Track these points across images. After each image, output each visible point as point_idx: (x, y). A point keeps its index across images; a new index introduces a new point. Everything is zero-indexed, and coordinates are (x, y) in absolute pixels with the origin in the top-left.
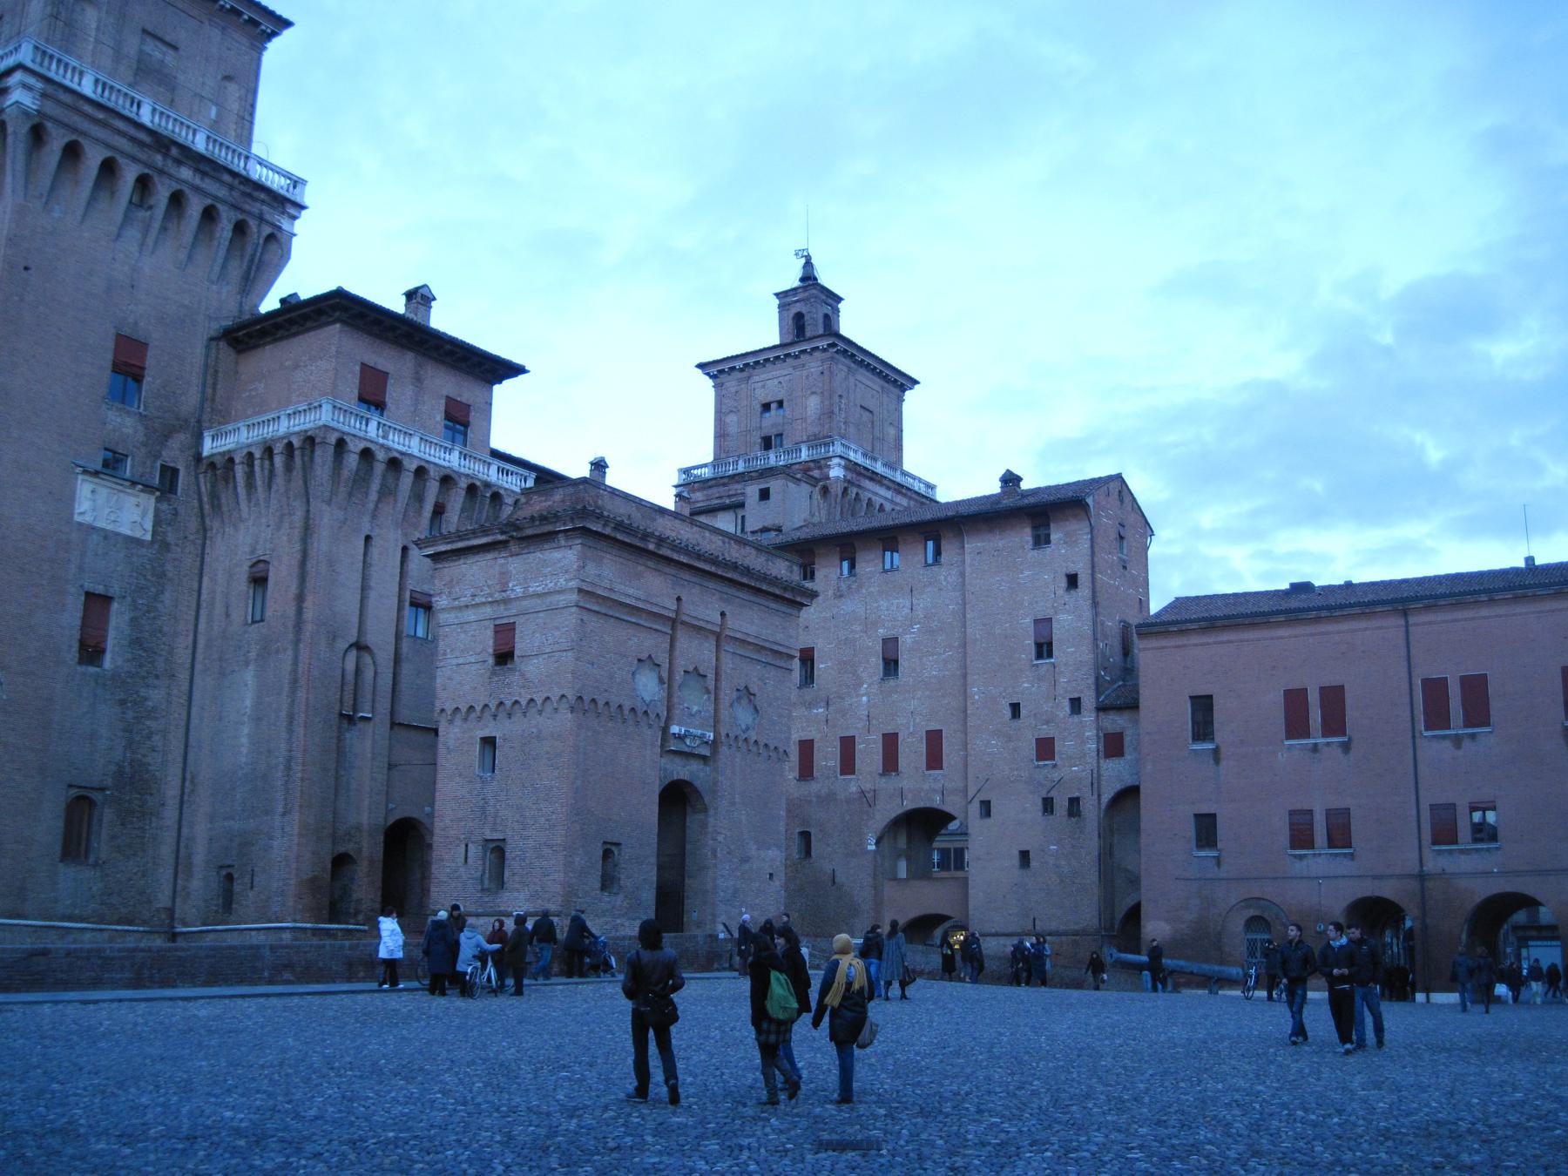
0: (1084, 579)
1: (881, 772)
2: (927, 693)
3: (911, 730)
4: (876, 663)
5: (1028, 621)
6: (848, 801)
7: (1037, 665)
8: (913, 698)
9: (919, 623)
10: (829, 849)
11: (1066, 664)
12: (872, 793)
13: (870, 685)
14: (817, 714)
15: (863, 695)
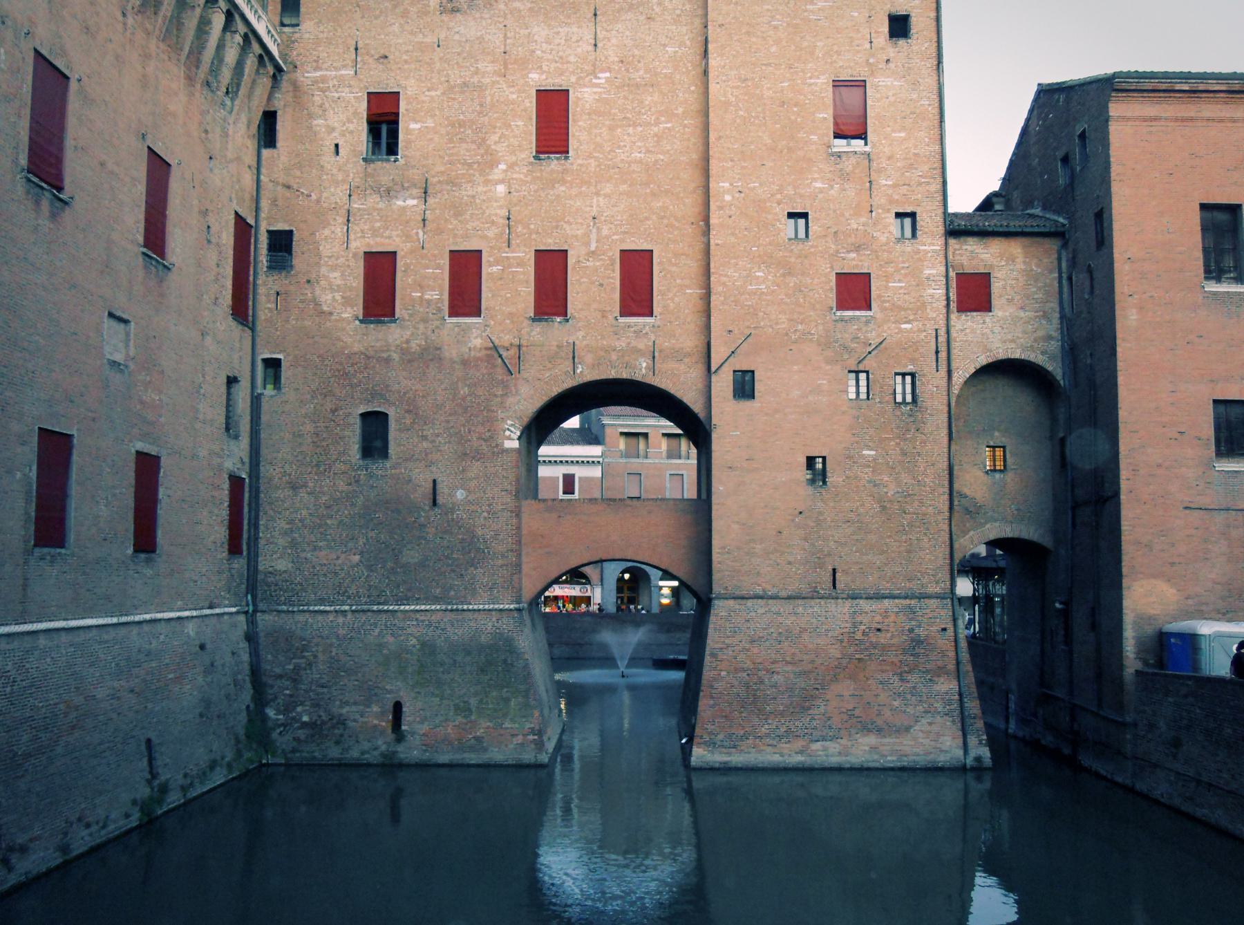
0: (920, 24)
1: (532, 315)
2: (624, 187)
3: (593, 247)
4: (525, 127)
5: (823, 82)
6: (465, 363)
7: (839, 155)
8: (597, 194)
9: (609, 70)
10: (425, 444)
11: (889, 158)
12: (513, 351)
13: (511, 166)
14: (404, 208)
15: (502, 181)
